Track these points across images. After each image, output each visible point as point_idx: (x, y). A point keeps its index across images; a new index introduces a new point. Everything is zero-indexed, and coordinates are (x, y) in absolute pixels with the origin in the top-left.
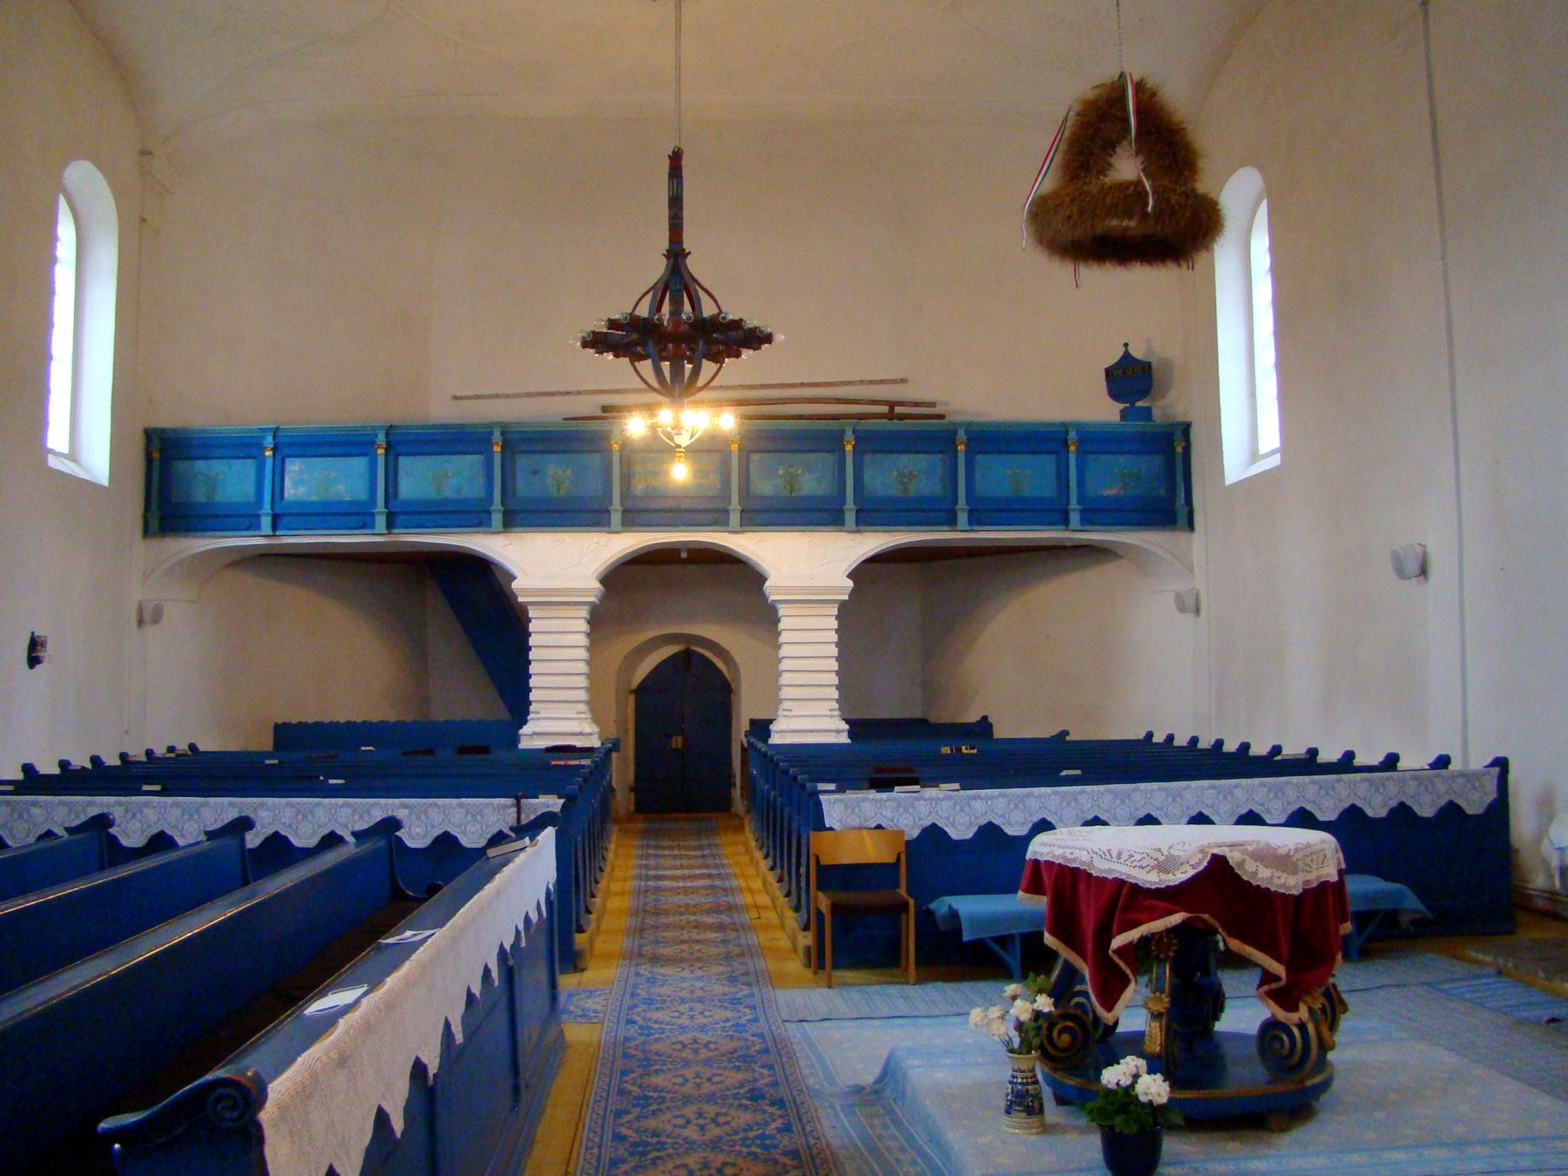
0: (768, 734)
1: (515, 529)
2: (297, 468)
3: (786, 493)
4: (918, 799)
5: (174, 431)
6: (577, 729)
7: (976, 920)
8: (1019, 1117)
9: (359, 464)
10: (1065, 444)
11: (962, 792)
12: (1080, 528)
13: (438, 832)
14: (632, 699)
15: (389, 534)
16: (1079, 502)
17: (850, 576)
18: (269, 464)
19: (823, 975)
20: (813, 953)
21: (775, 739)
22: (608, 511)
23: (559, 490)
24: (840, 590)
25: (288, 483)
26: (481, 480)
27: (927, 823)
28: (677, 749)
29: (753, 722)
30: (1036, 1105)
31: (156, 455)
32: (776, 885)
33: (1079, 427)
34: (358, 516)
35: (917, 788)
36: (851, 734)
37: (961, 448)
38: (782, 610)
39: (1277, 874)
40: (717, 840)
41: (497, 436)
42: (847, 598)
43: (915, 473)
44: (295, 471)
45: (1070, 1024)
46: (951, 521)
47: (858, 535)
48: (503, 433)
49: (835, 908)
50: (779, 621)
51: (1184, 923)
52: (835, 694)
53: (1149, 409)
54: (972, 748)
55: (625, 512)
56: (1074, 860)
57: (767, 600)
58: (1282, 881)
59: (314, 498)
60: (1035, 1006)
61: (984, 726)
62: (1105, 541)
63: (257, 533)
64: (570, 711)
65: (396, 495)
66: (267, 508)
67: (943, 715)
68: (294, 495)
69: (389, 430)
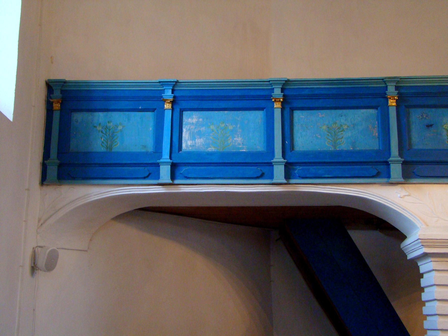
2: (194, 121)
5: (76, 83)
25: (185, 135)
31: (57, 106)
44: (193, 124)
59: (211, 149)
66: (166, 156)
68: (192, 146)
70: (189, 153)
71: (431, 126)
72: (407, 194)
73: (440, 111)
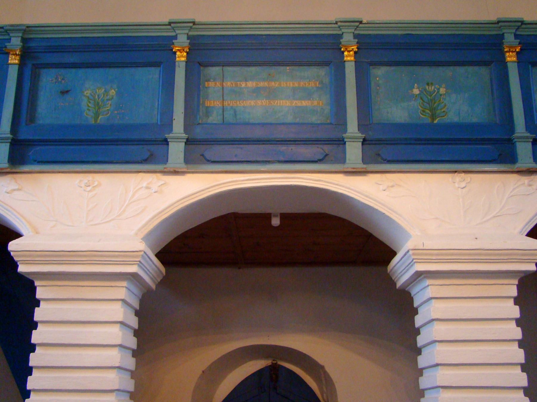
1: (26, 168)
3: (426, 119)
23: (97, 115)
41: (16, 42)
48: (24, 40)
57: (394, 284)
71: (67, 92)
72: (17, 187)
73: (81, 72)
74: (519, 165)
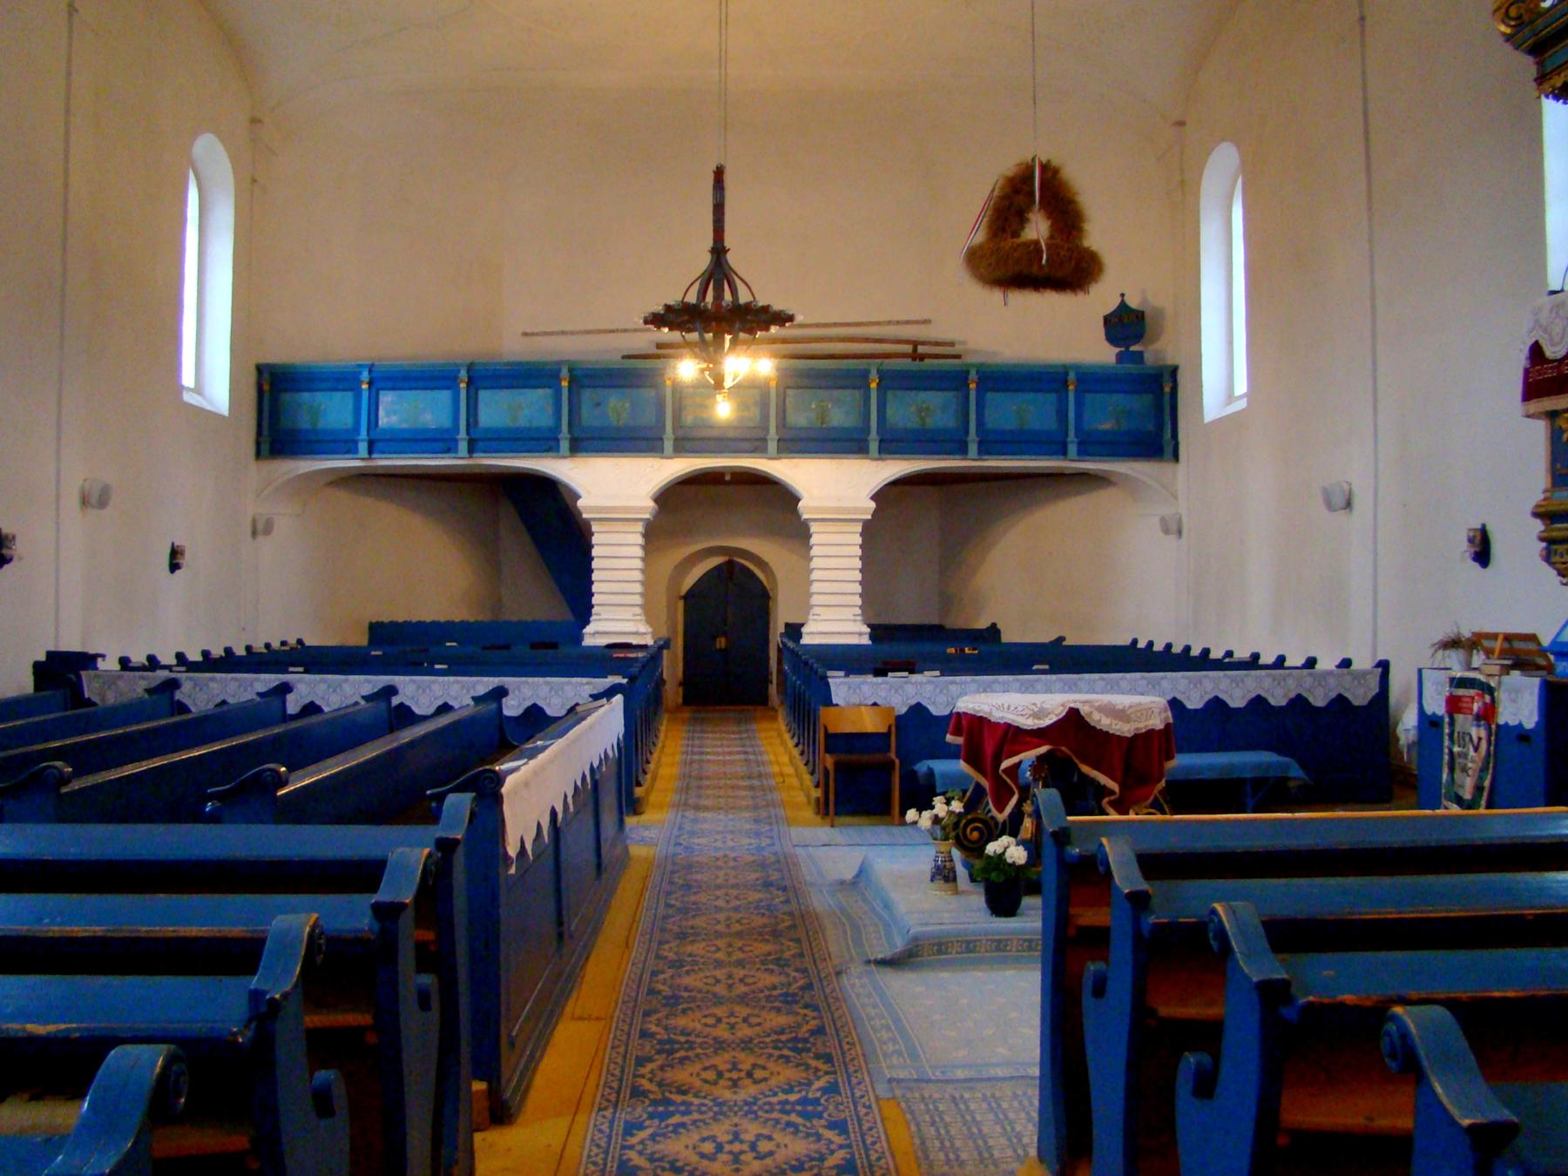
0: (800, 636)
1: (579, 454)
3: (819, 425)
4: (906, 683)
5: (283, 366)
6: (634, 630)
7: (944, 775)
8: (940, 883)
9: (444, 396)
10: (1065, 383)
11: (941, 678)
12: (1077, 458)
13: (528, 703)
14: (681, 604)
15: (471, 457)
16: (1076, 436)
17: (874, 498)
18: (365, 395)
19: (828, 820)
20: (822, 800)
21: (806, 640)
22: (662, 439)
23: (618, 421)
24: (863, 511)
25: (381, 413)
26: (550, 410)
27: (913, 702)
28: (720, 649)
29: (787, 625)
30: (951, 875)
31: (266, 387)
32: (798, 757)
33: (1077, 368)
34: (442, 441)
35: (906, 674)
36: (872, 637)
37: (973, 386)
38: (814, 528)
39: (1114, 722)
40: (755, 727)
41: (565, 372)
42: (869, 517)
43: (932, 407)
45: (979, 825)
46: (962, 450)
47: (880, 462)
48: (571, 370)
49: (837, 764)
50: (811, 536)
51: (1048, 753)
52: (858, 601)
53: (1141, 353)
54: (974, 649)
55: (676, 440)
56: (980, 711)
58: (1118, 727)
59: (405, 426)
60: (951, 808)
61: (994, 631)
62: (1100, 470)
63: (355, 456)
64: (628, 613)
65: (476, 422)
66: (363, 434)
67: (955, 622)
69: (470, 367)
70: (385, 431)
74: (871, 455)
